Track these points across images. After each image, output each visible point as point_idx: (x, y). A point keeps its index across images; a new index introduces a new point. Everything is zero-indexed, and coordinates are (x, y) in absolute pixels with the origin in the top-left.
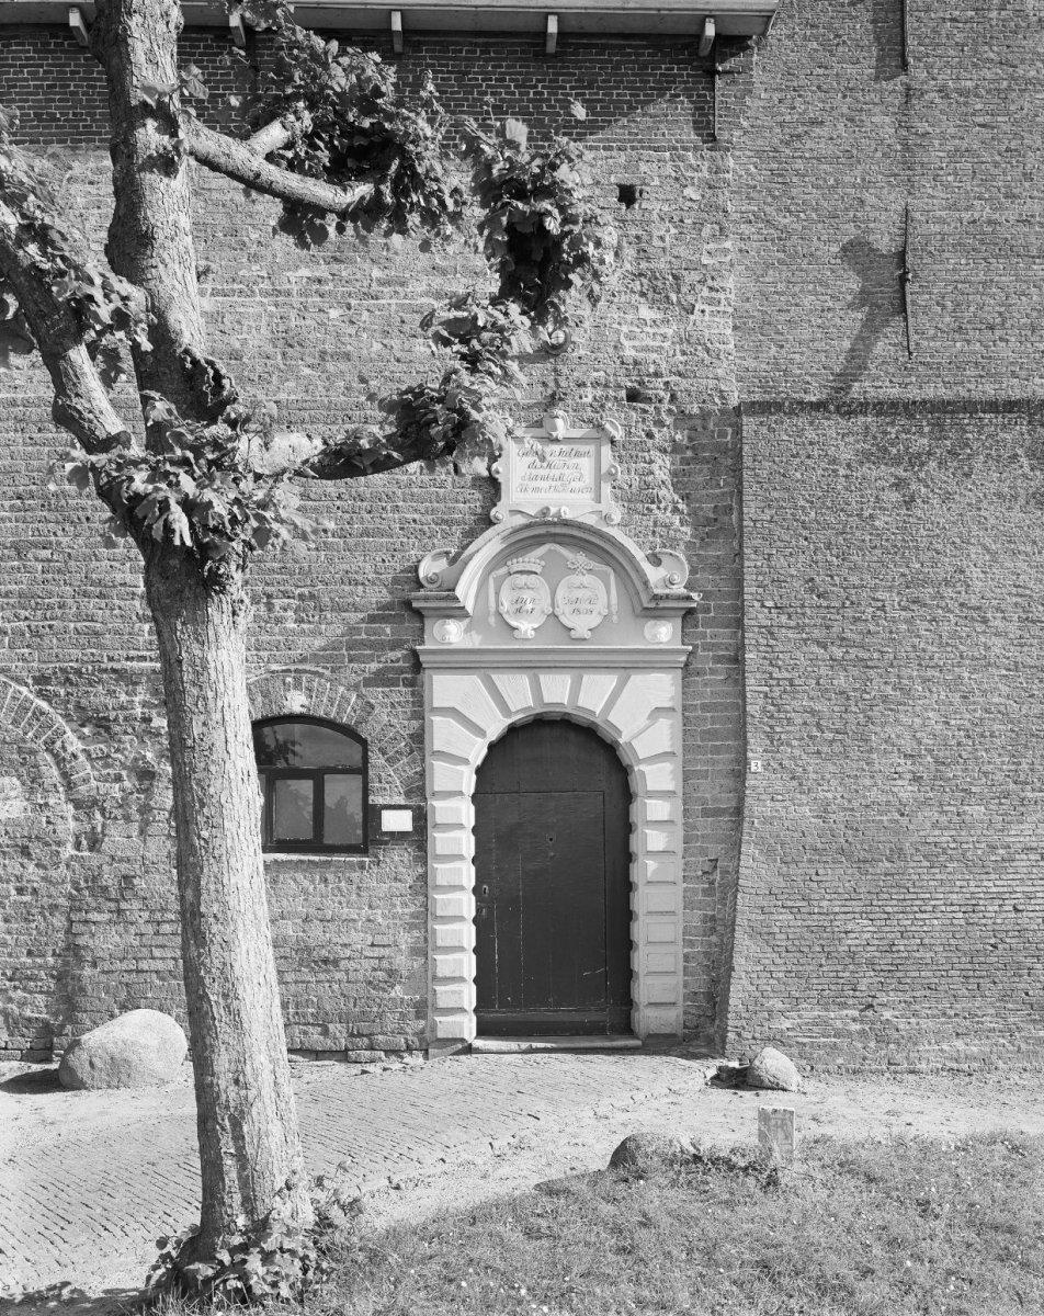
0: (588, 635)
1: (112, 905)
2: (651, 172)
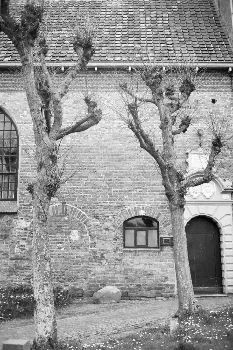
0: (209, 197)
1: (99, 261)
2: (218, 97)
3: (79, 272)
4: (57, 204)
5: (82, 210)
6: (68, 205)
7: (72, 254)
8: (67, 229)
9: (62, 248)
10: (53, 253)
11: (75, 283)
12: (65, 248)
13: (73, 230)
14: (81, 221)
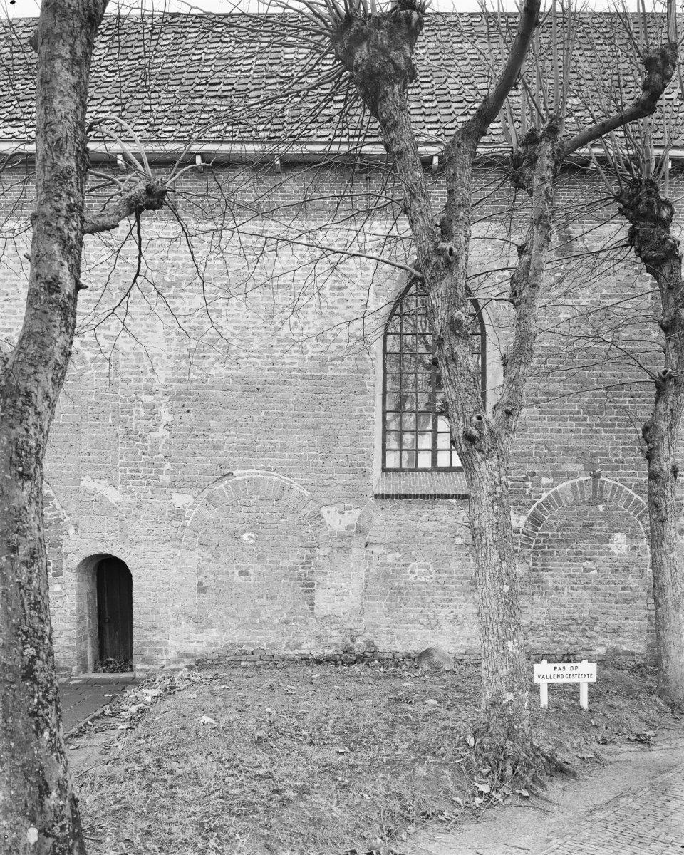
3: (626, 618)
4: (582, 479)
5: (634, 491)
6: (606, 479)
7: (614, 583)
8: (602, 530)
9: (593, 570)
10: (574, 580)
11: (620, 639)
12: (598, 571)
13: (615, 532)
14: (632, 513)
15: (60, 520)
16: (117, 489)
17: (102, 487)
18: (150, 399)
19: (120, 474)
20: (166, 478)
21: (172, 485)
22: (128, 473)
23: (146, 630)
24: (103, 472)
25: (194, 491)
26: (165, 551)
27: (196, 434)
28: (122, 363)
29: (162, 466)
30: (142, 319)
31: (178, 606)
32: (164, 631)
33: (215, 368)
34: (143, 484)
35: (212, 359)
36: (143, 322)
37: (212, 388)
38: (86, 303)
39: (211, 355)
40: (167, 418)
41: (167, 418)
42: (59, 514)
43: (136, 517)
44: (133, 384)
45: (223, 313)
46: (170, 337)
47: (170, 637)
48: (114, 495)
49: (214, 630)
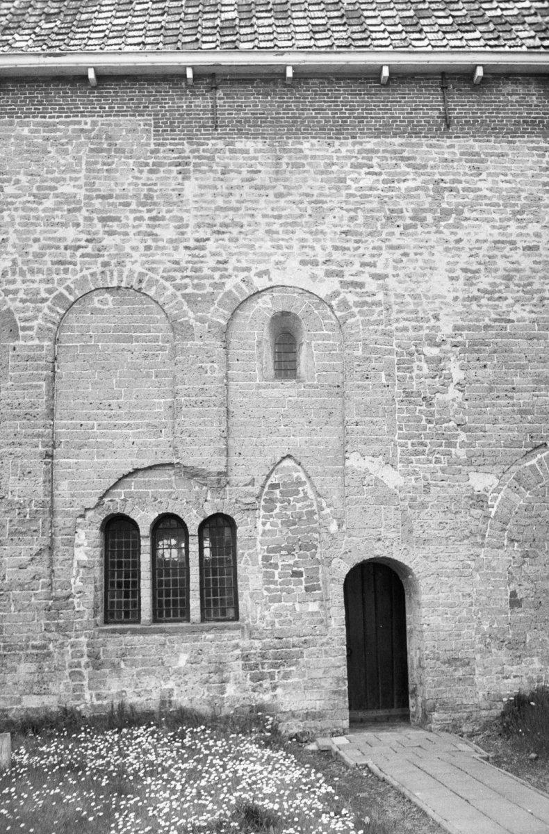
15: (312, 513)
16: (396, 469)
17: (374, 467)
18: (434, 352)
19: (399, 449)
20: (461, 453)
21: (469, 463)
22: (410, 447)
23: (444, 663)
24: (376, 447)
25: (497, 470)
26: (464, 549)
27: (498, 394)
28: (395, 308)
29: (457, 436)
30: (416, 254)
31: (485, 627)
32: (468, 664)
33: (515, 312)
34: (431, 462)
35: (510, 301)
36: (418, 257)
37: (514, 336)
38: (343, 235)
39: (509, 295)
40: (458, 375)
41: (458, 375)
42: (311, 505)
43: (423, 505)
44: (411, 333)
45: (520, 245)
46: (454, 275)
47: (477, 672)
48: (392, 478)
49: (536, 659)
